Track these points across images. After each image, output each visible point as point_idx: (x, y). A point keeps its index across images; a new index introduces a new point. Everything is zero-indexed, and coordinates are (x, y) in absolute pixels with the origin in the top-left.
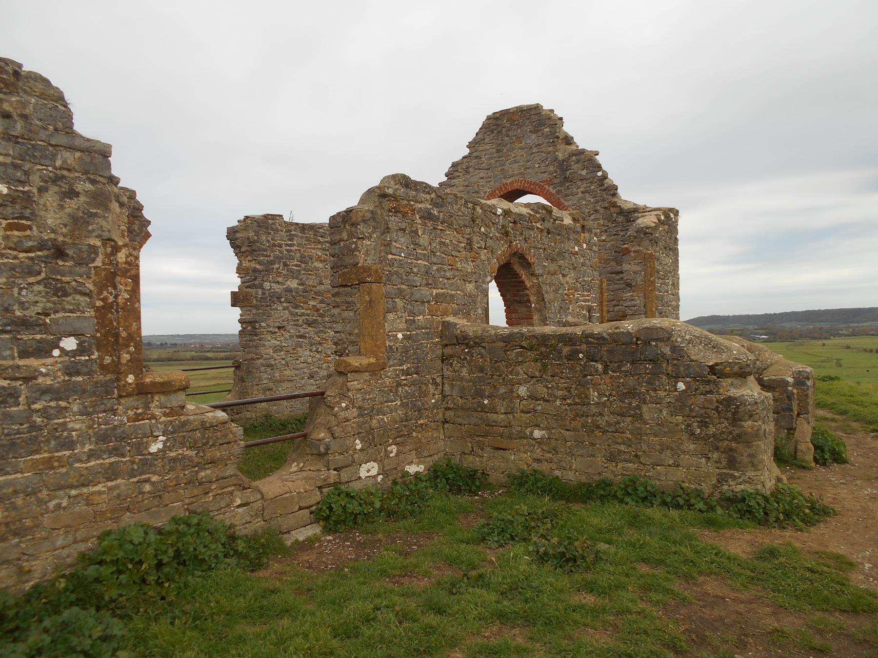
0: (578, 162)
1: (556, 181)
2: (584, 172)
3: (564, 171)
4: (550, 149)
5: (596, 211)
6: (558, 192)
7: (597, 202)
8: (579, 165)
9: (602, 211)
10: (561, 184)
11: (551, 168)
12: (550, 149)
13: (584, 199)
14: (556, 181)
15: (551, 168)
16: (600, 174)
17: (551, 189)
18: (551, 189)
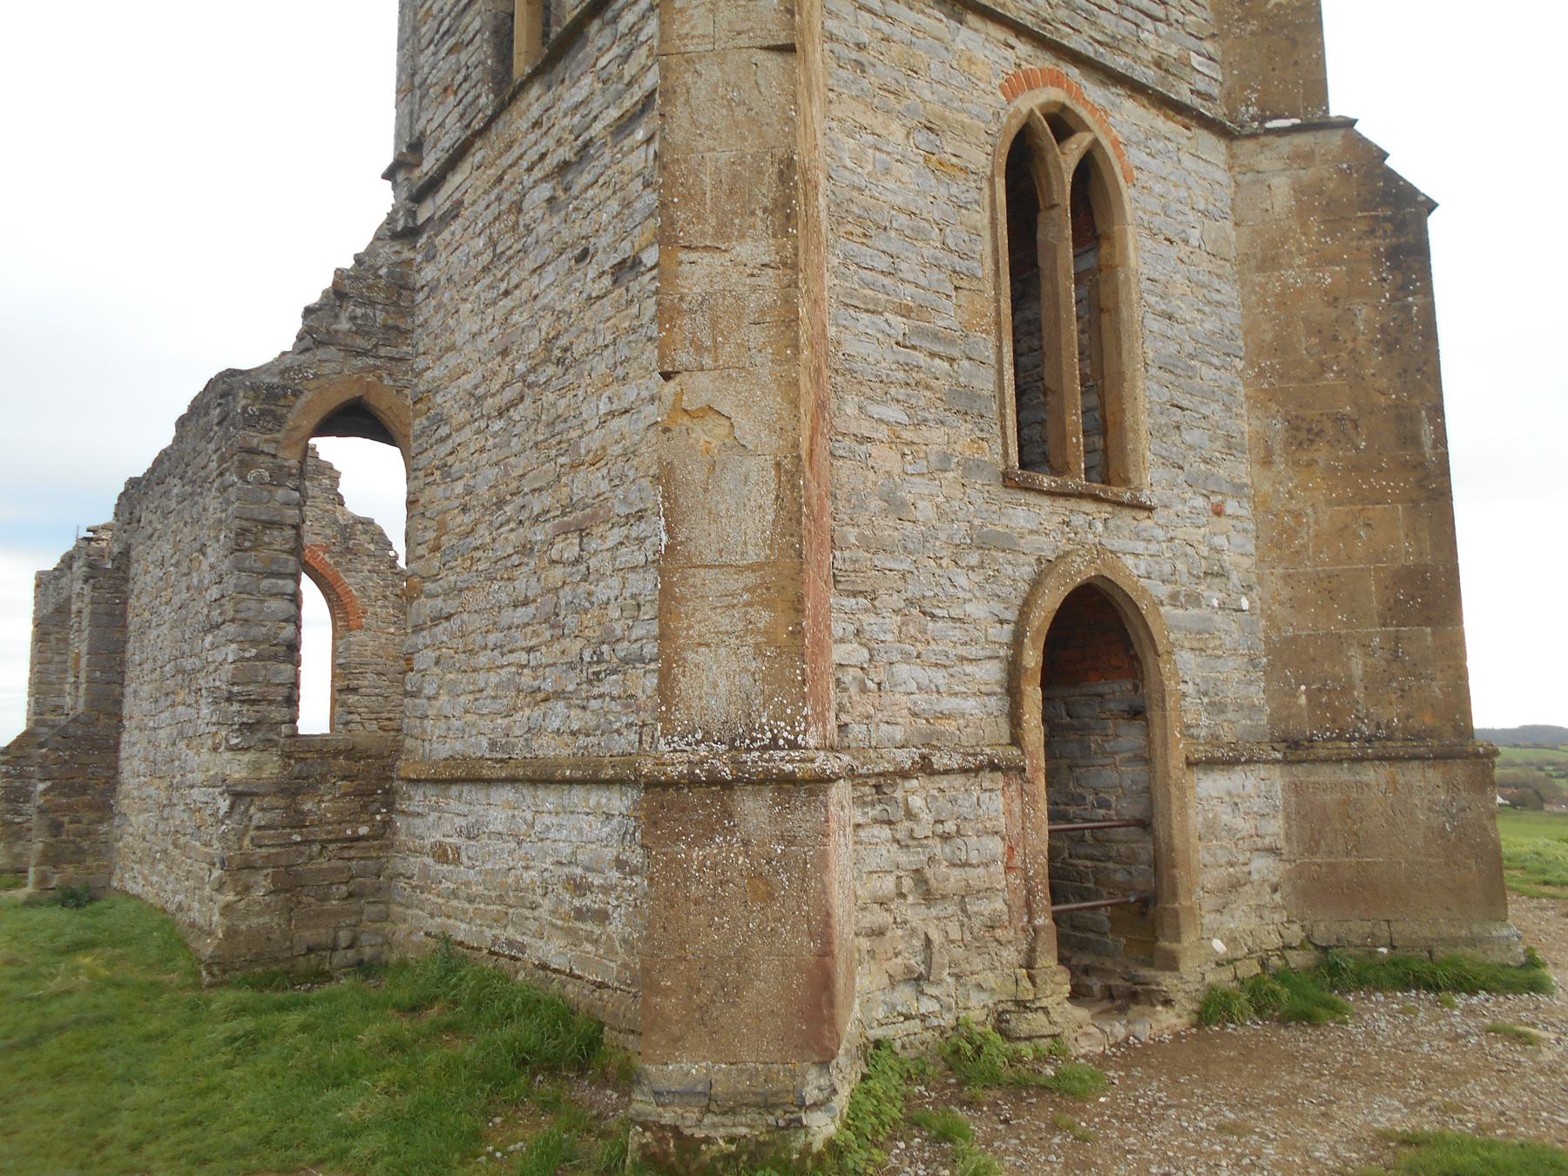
0: (366, 532)
1: (333, 548)
2: (372, 547)
3: (346, 539)
4: (330, 507)
5: (385, 597)
6: (337, 564)
7: (387, 586)
8: (367, 537)
9: (392, 598)
10: (342, 554)
11: (328, 532)
12: (330, 507)
13: (371, 579)
14: (333, 548)
15: (328, 532)
16: (392, 553)
17: (327, 557)
18: (327, 557)
